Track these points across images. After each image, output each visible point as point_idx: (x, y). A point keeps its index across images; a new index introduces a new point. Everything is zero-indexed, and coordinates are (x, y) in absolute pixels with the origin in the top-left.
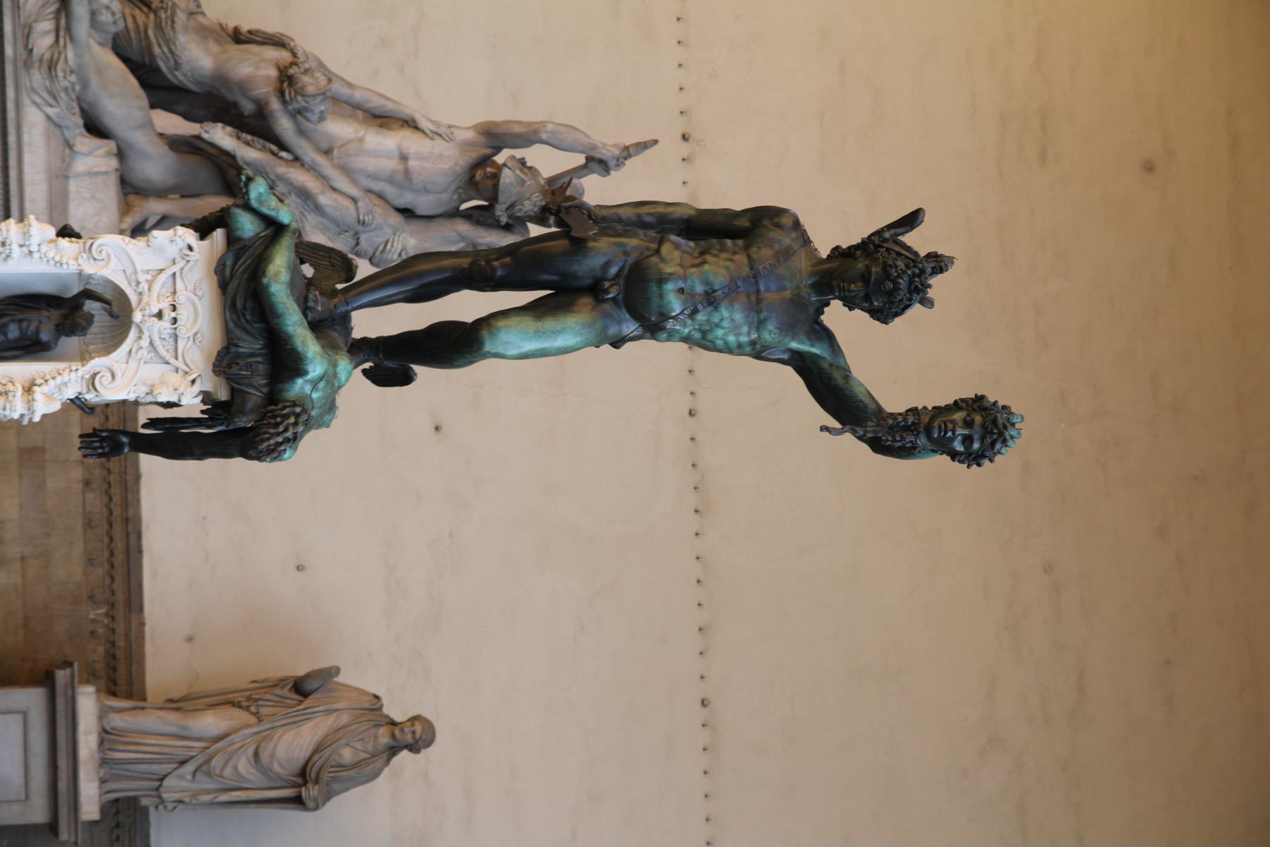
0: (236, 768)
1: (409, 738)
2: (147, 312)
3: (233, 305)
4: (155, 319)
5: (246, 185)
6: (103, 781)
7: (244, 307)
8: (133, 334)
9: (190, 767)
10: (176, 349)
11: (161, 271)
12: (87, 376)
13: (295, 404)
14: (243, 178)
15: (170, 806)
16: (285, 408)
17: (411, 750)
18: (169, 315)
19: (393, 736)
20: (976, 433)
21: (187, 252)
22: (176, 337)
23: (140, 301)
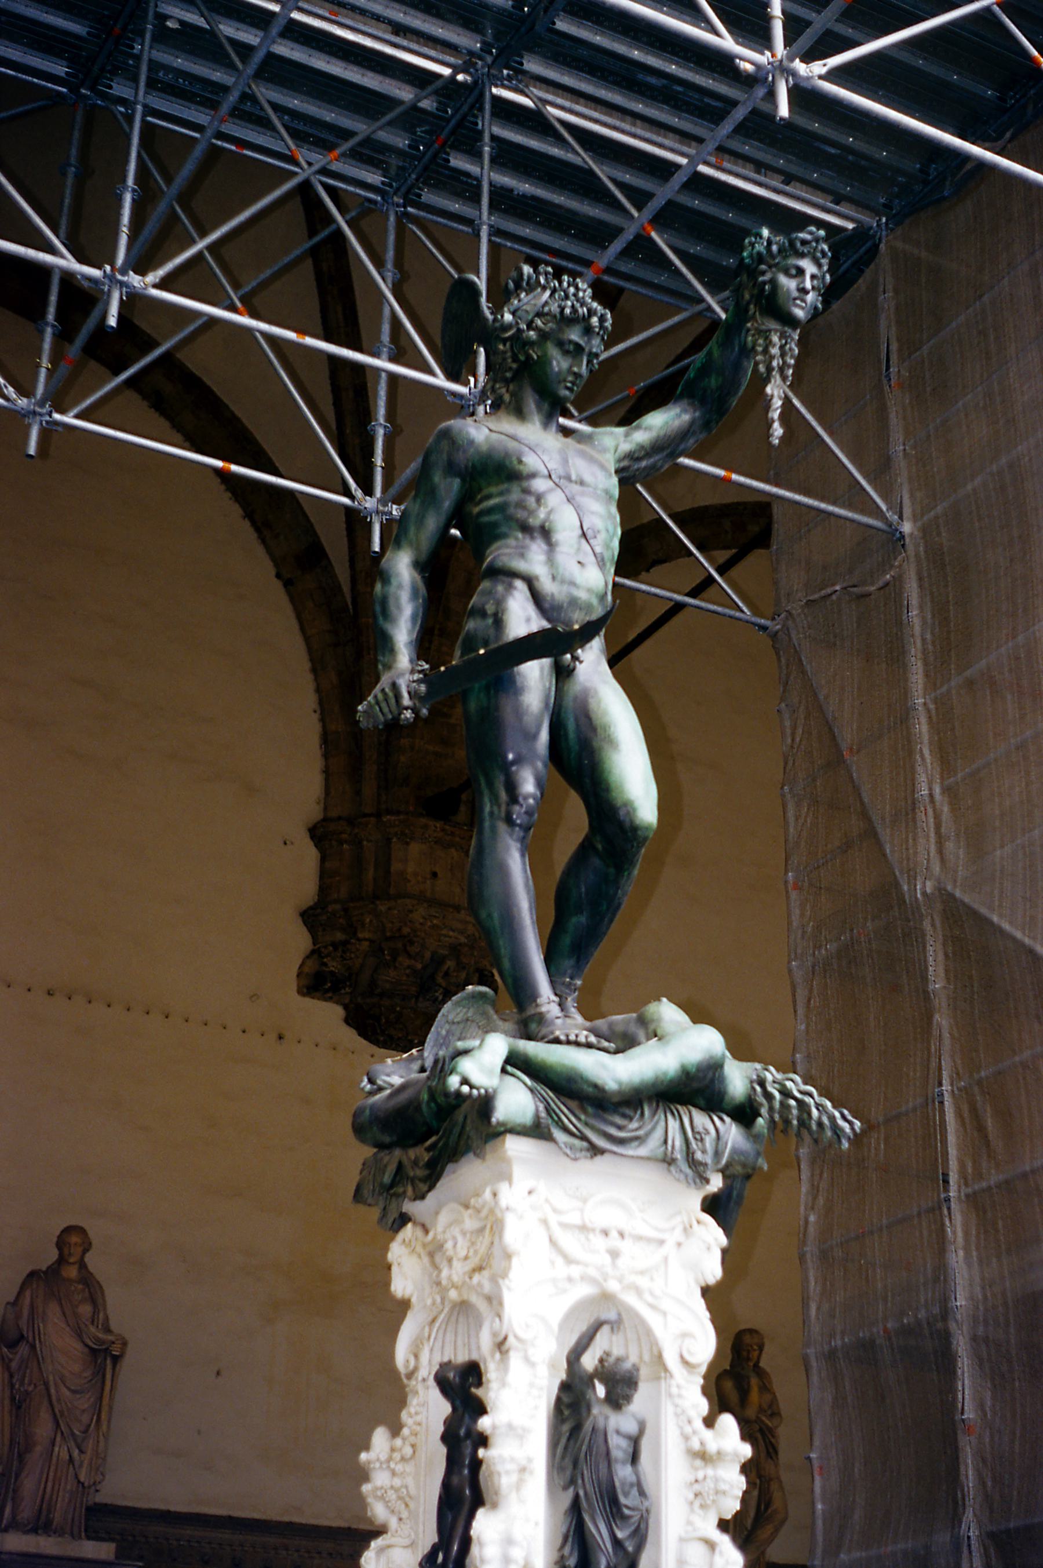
0: (84, 1411)
1: (80, 1249)
2: (609, 1270)
3: (621, 1142)
4: (620, 1262)
5: (472, 1087)
6: (80, 1538)
7: (620, 1128)
8: (631, 1299)
9: (76, 1453)
10: (649, 1240)
11: (552, 1241)
12: (685, 1372)
13: (762, 1083)
14: (465, 1089)
15: (99, 1478)
16: (769, 1096)
17: (88, 1250)
18: (614, 1241)
19: (73, 1264)
20: (809, 267)
21: (533, 1197)
22: (639, 1238)
23: (593, 1281)
